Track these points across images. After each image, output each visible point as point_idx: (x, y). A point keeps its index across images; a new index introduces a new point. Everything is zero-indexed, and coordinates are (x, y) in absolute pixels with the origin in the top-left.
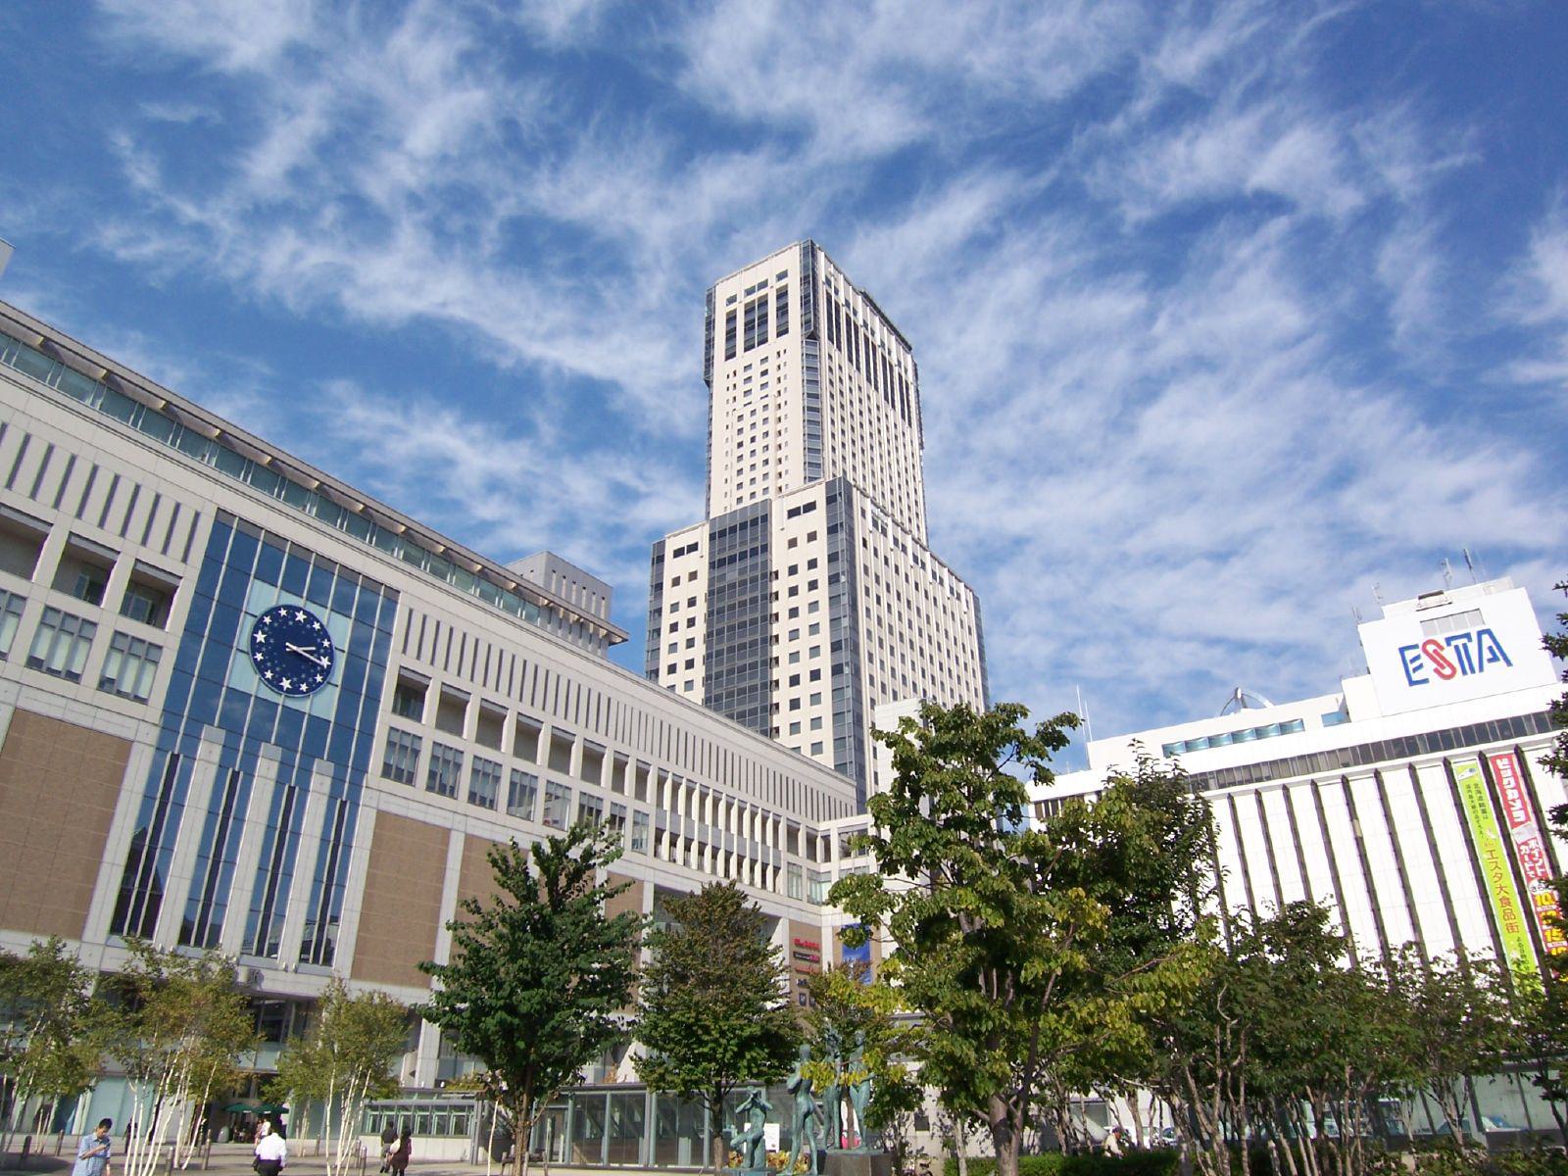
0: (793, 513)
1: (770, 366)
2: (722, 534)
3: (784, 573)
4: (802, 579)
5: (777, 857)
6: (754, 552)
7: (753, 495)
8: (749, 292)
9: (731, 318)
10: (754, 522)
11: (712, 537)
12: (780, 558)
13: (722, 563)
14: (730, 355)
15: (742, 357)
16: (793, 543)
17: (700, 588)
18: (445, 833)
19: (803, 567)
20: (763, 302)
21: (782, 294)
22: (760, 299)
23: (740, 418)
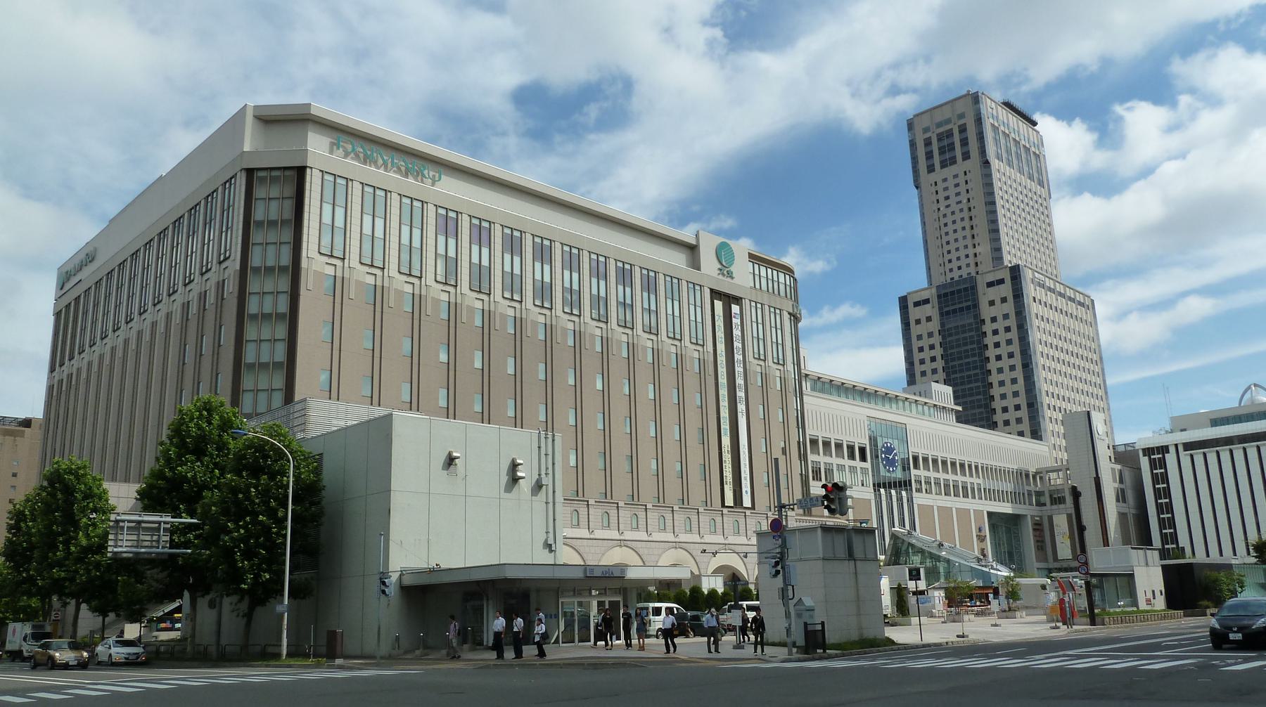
0: (990, 285)
1: (961, 180)
2: (946, 295)
3: (988, 321)
4: (1000, 325)
5: (1023, 489)
6: (968, 308)
7: (960, 268)
8: (939, 125)
9: (928, 143)
10: (966, 289)
11: (939, 297)
12: (986, 312)
13: (948, 313)
14: (931, 169)
15: (939, 174)
16: (992, 303)
17: (935, 326)
18: (933, 506)
19: (1000, 318)
20: (950, 134)
21: (963, 129)
22: (947, 131)
23: (945, 216)
